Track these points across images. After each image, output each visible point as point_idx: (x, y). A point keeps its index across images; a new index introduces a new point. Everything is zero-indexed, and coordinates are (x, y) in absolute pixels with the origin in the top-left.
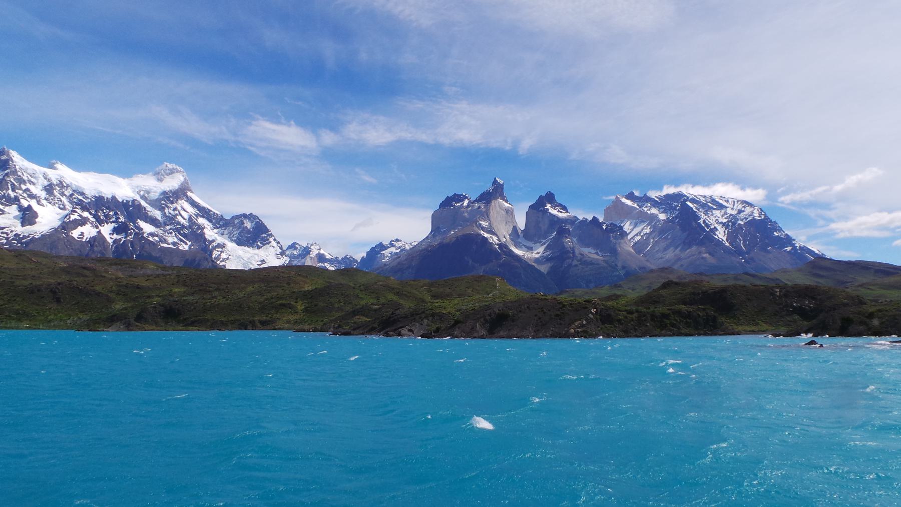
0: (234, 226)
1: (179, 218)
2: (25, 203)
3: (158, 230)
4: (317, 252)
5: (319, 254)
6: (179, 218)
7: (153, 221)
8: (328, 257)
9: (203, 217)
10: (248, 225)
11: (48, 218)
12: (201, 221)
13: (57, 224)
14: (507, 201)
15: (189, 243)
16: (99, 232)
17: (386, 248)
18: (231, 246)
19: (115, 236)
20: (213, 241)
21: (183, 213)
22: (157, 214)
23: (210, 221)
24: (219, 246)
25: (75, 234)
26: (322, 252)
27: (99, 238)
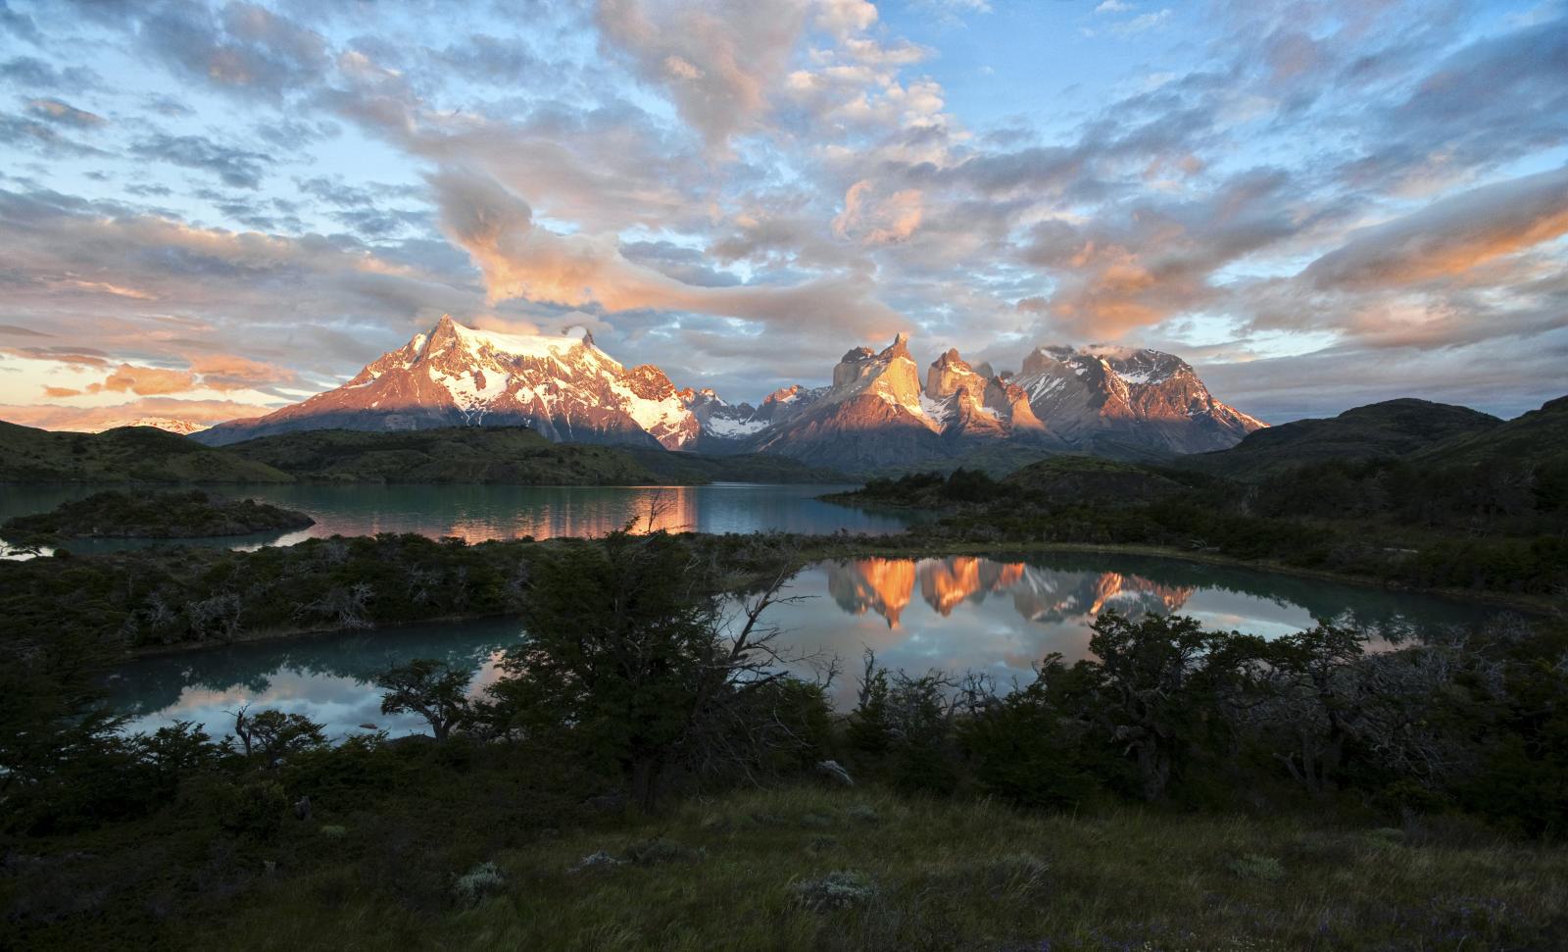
0: (635, 377)
1: (588, 372)
2: (475, 369)
3: (569, 385)
4: (711, 399)
5: (714, 400)
6: (588, 373)
7: (566, 378)
8: (723, 404)
9: (605, 369)
10: (650, 376)
11: (496, 382)
12: (605, 374)
13: (504, 387)
14: (909, 359)
15: (598, 398)
16: (535, 394)
17: (787, 395)
18: (634, 397)
19: (548, 397)
20: (619, 395)
21: (591, 368)
22: (568, 370)
23: (612, 374)
24: (624, 400)
25: (519, 395)
26: (717, 399)
27: (537, 400)
